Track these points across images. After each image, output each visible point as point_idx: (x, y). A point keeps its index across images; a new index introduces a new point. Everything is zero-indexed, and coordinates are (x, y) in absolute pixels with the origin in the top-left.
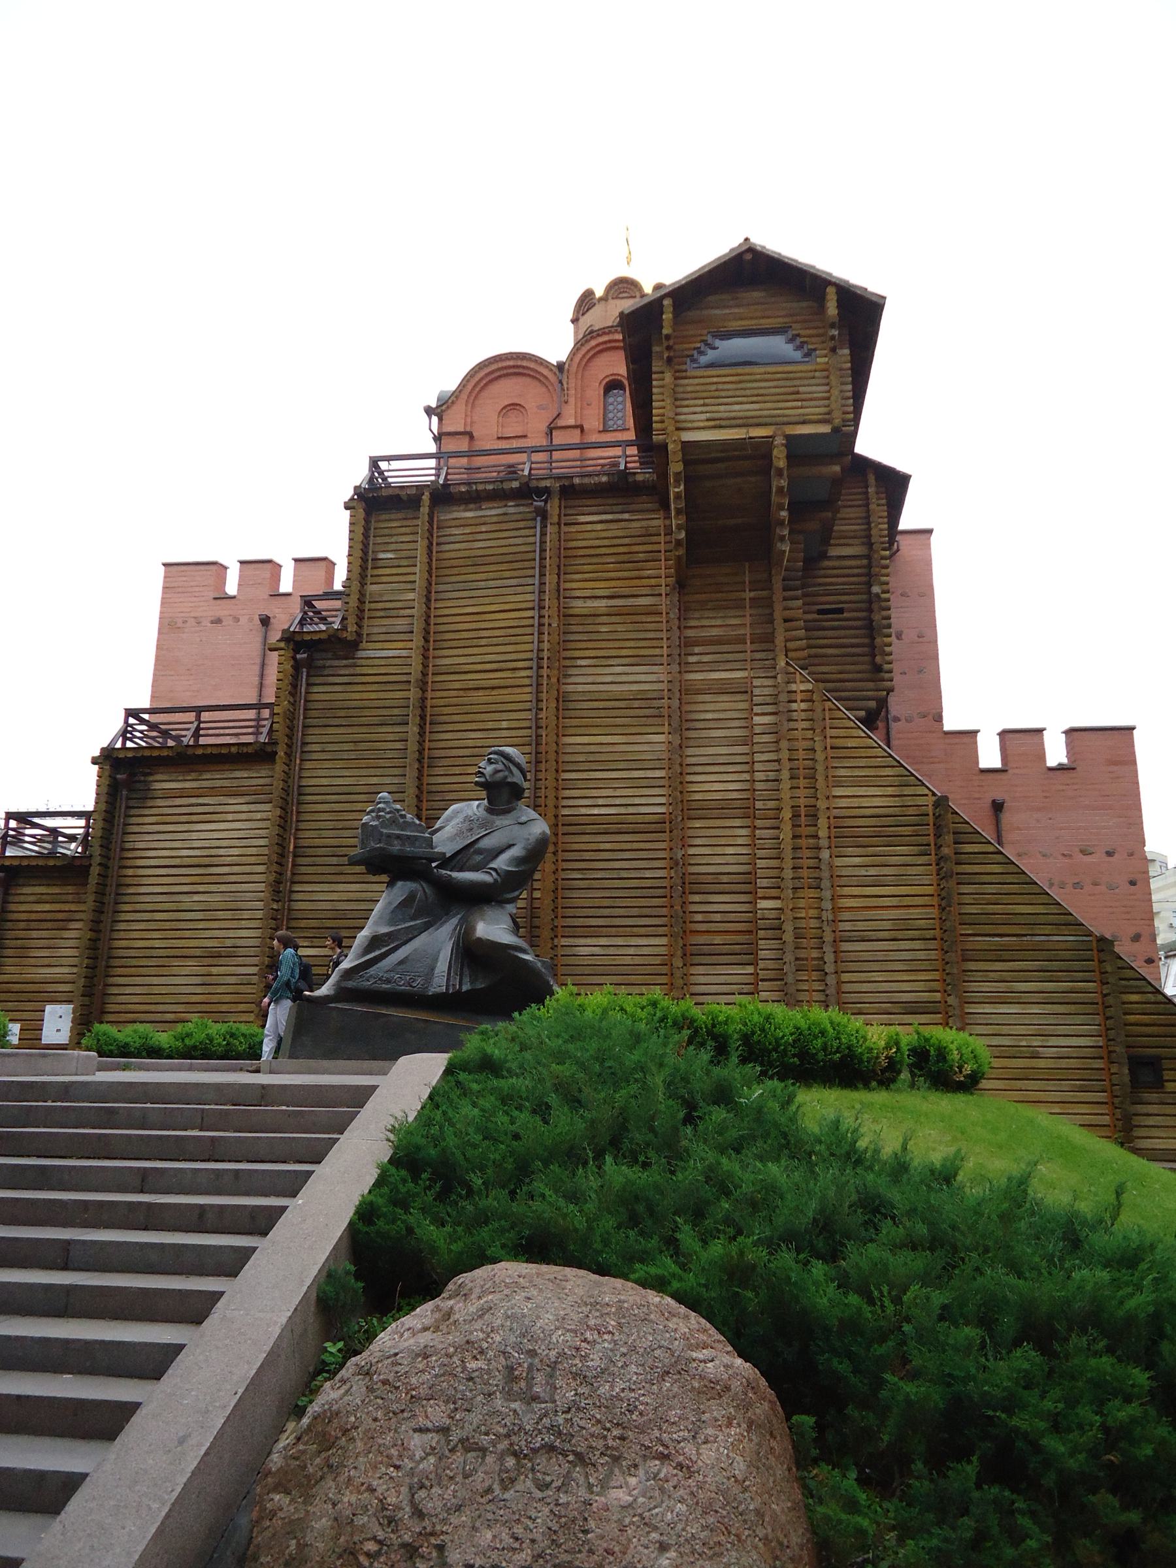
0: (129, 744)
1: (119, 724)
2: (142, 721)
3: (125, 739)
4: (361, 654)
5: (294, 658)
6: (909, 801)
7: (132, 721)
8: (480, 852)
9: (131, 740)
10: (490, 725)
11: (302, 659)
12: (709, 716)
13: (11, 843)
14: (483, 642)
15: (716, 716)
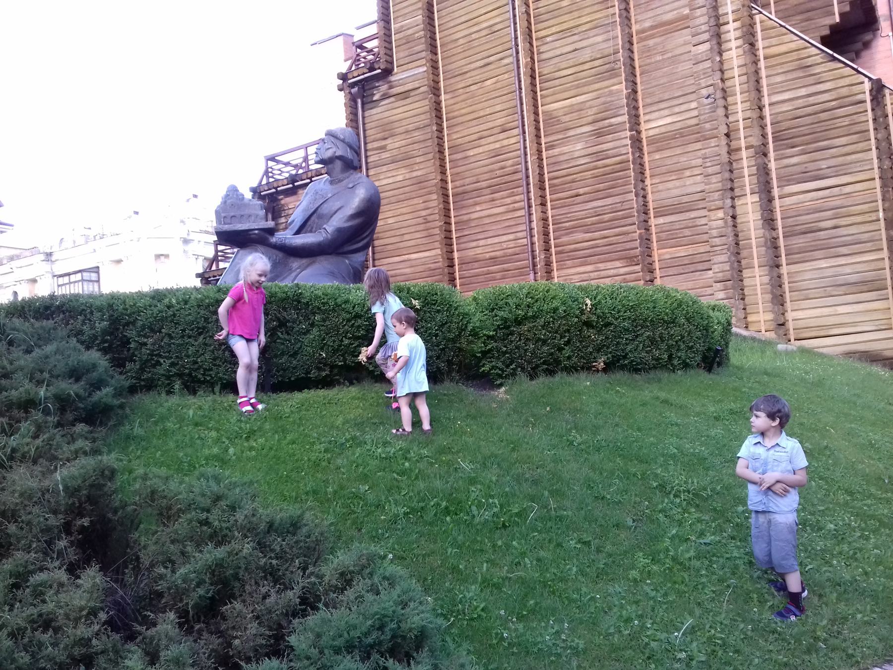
0: (271, 180)
1: (263, 169)
2: (278, 162)
3: (268, 177)
4: (392, 78)
5: (350, 93)
6: (844, 91)
7: (271, 163)
8: (320, 217)
9: (272, 177)
10: (488, 111)
11: (355, 93)
12: (659, 58)
13: (221, 261)
14: (475, 43)
15: (665, 57)
